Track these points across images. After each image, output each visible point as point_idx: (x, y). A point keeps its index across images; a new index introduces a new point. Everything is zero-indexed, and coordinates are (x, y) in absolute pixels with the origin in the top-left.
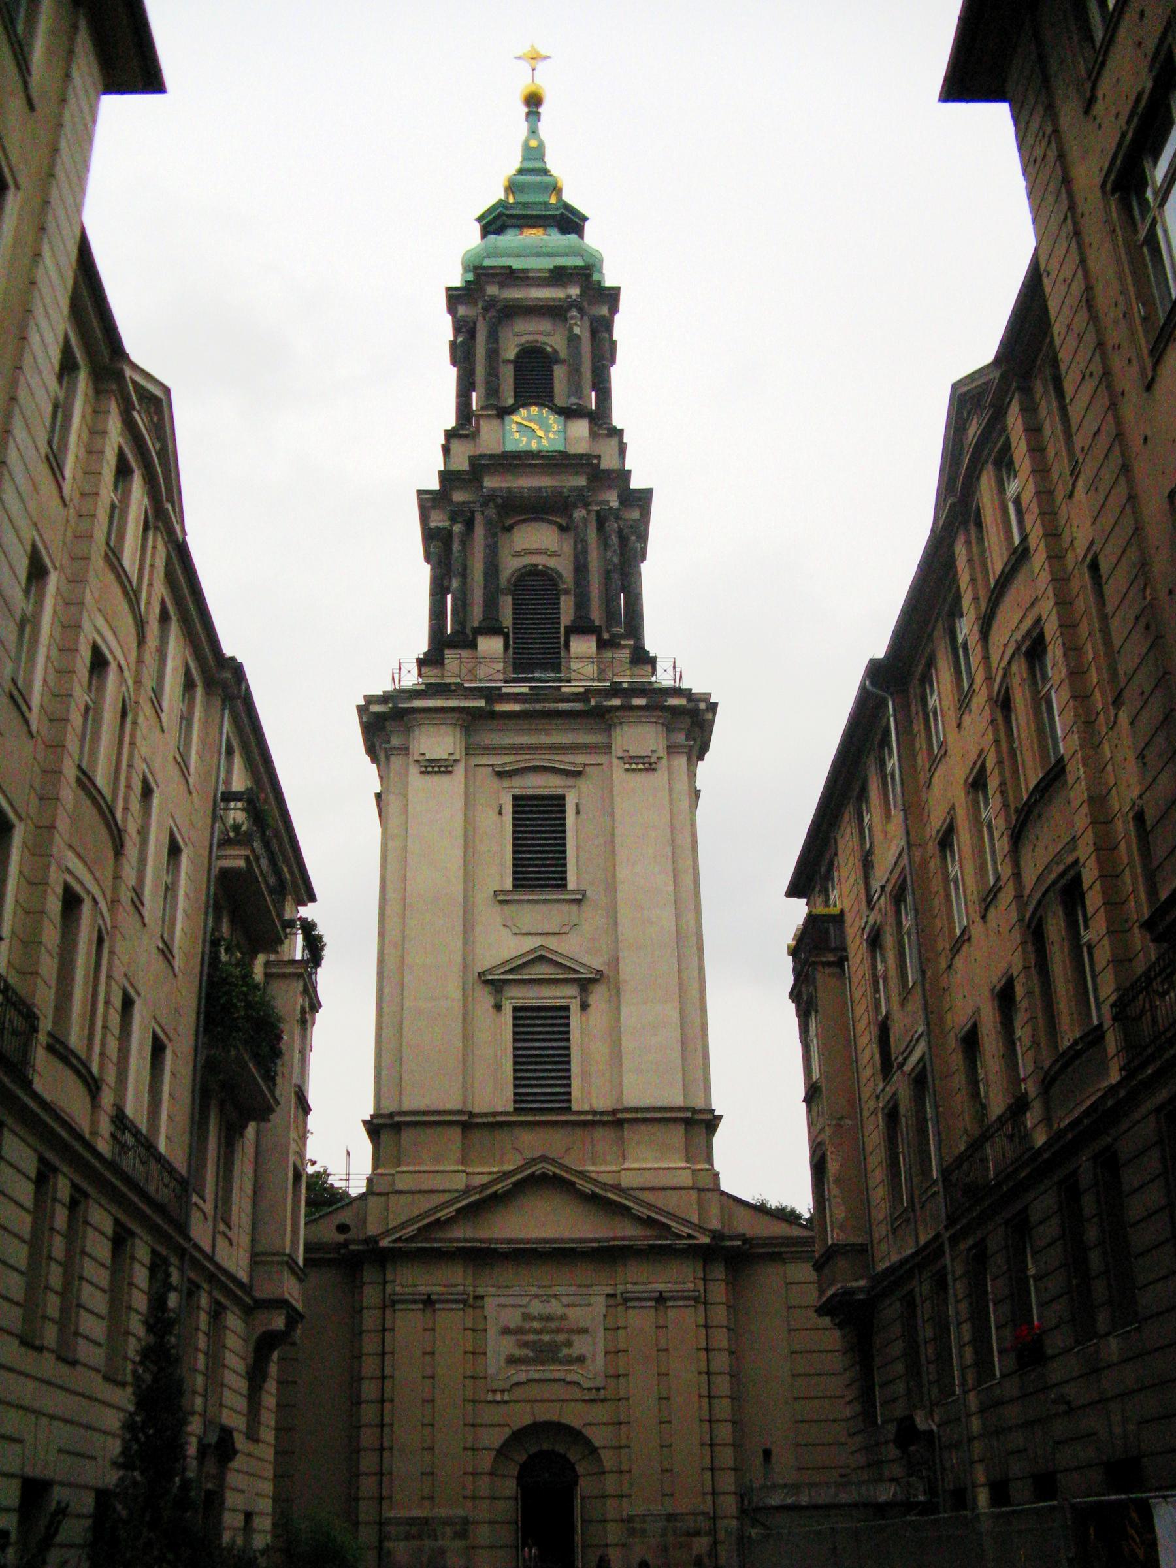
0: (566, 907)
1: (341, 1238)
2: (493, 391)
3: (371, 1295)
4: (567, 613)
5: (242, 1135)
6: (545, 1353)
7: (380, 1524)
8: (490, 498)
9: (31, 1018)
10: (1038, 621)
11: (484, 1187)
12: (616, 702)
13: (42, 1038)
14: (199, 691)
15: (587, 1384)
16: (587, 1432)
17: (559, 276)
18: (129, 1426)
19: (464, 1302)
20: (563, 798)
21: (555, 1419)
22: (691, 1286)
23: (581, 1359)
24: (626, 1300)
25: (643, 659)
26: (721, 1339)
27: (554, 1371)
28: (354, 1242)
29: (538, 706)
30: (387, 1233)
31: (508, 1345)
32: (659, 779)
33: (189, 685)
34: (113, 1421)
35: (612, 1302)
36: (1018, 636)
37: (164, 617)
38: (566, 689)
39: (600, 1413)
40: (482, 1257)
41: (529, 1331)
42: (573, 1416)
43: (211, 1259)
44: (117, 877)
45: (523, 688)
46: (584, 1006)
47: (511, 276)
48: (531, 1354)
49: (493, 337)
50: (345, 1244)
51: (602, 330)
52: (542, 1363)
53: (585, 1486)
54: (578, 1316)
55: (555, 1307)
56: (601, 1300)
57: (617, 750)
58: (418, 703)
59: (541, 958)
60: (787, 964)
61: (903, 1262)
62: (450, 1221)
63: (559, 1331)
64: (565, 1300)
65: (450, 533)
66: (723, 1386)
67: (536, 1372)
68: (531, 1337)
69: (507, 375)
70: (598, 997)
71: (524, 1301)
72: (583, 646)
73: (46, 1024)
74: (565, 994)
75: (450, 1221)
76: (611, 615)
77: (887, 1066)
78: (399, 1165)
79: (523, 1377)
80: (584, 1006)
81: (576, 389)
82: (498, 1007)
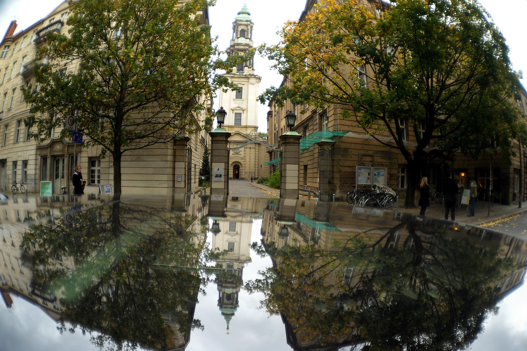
2: (237, 35)
8: (236, 49)
17: (247, 21)
25: (253, 70)
26: (257, 153)
27: (238, 156)
32: (254, 86)
38: (244, 74)
39: (243, 160)
42: (240, 161)
45: (238, 74)
47: (241, 21)
49: (237, 28)
51: (252, 27)
53: (241, 168)
60: (267, 115)
66: (257, 158)
69: (239, 33)
70: (245, 112)
72: (246, 68)
76: (250, 65)
77: (275, 129)
81: (248, 35)
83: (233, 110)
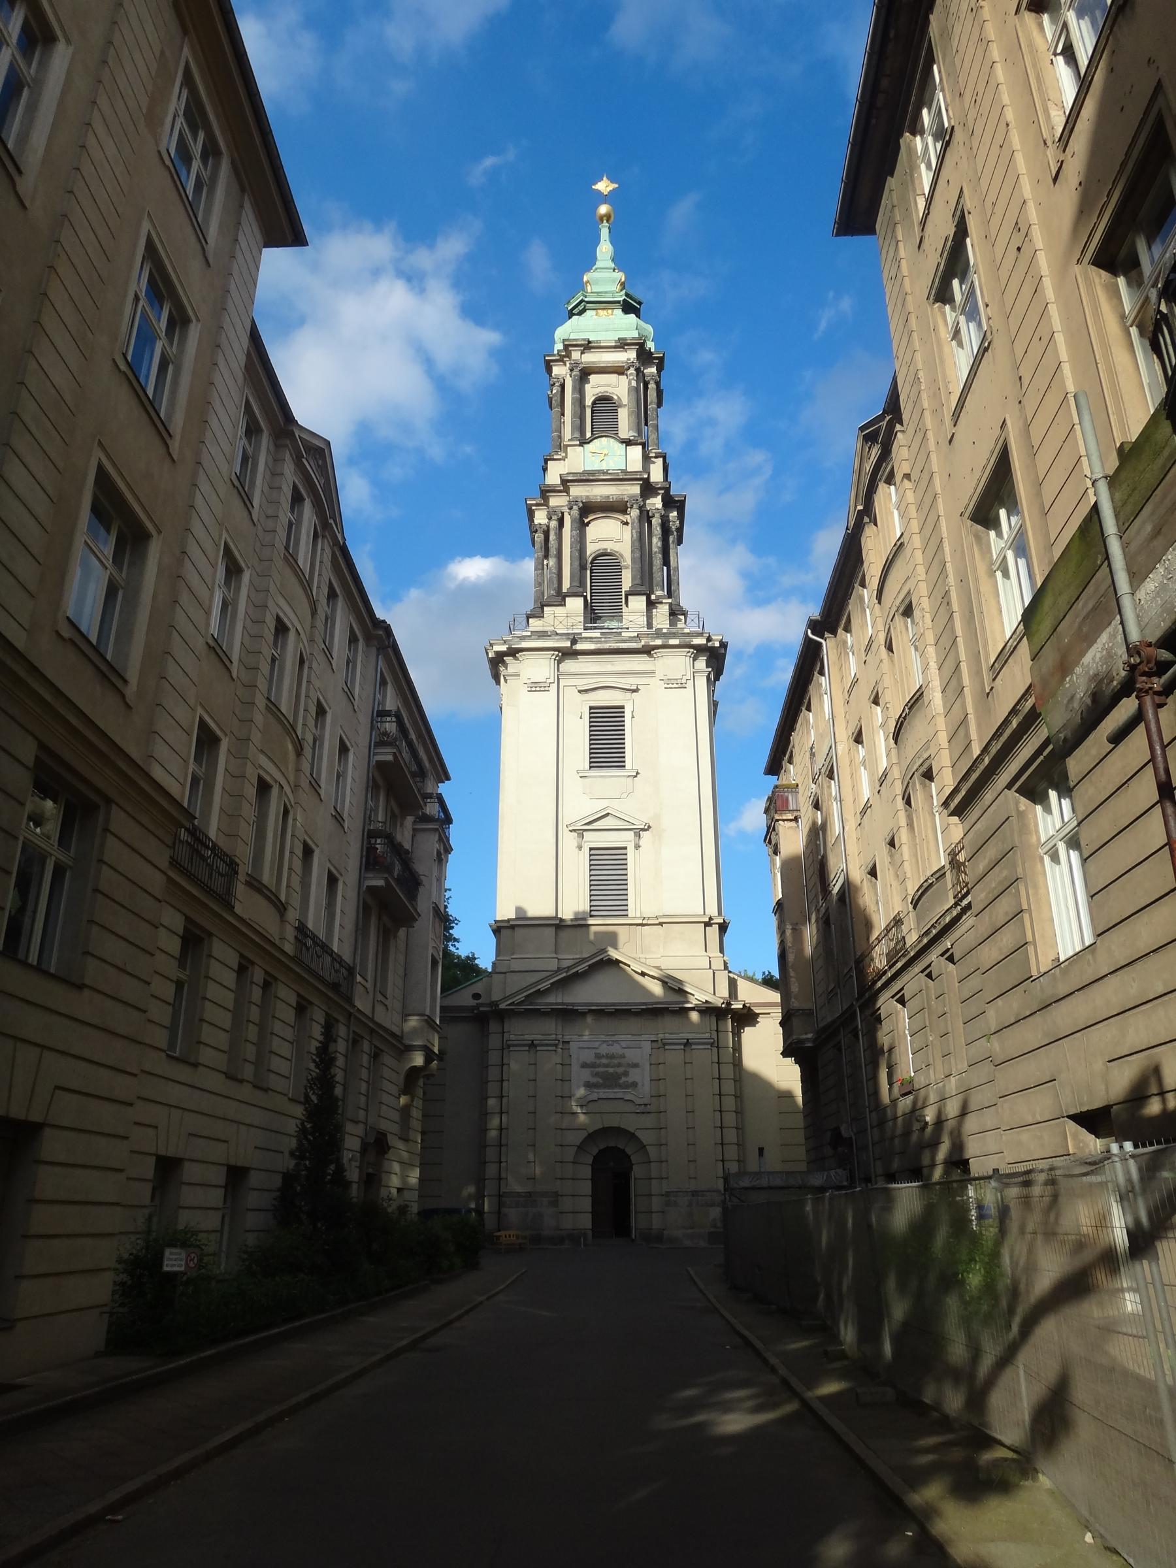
0: (624, 780)
1: (474, 1002)
3: (494, 1041)
4: (627, 583)
5: (395, 937)
6: (611, 1080)
7: (500, 1196)
9: (233, 866)
10: (909, 592)
11: (569, 968)
12: (659, 642)
13: (242, 877)
14: (361, 644)
15: (638, 1101)
16: (639, 1134)
18: (303, 1131)
19: (556, 1045)
20: (623, 707)
21: (615, 1124)
22: (707, 1035)
23: (634, 1085)
24: (664, 1045)
27: (618, 1093)
28: (482, 1005)
29: (606, 646)
30: (505, 999)
31: (586, 1075)
33: (353, 639)
34: (292, 1126)
35: (655, 1045)
36: (898, 602)
37: (332, 595)
39: (649, 1121)
40: (569, 1014)
41: (599, 1066)
42: (629, 1123)
43: (372, 1020)
44: (298, 770)
45: (596, 634)
46: (637, 847)
47: (588, 346)
48: (601, 1081)
50: (479, 1005)
52: (609, 1087)
53: (637, 1171)
54: (632, 1055)
55: (616, 1049)
56: (647, 1046)
57: (659, 674)
58: (524, 645)
59: (608, 814)
61: (834, 1022)
62: (547, 991)
63: (619, 1065)
64: (624, 1044)
65: (548, 527)
67: (603, 1093)
68: (601, 1070)
71: (596, 1044)
73: (244, 869)
74: (625, 839)
75: (547, 991)
78: (513, 954)
79: (594, 1096)
80: (637, 847)
82: (580, 848)
83: (580, 833)
